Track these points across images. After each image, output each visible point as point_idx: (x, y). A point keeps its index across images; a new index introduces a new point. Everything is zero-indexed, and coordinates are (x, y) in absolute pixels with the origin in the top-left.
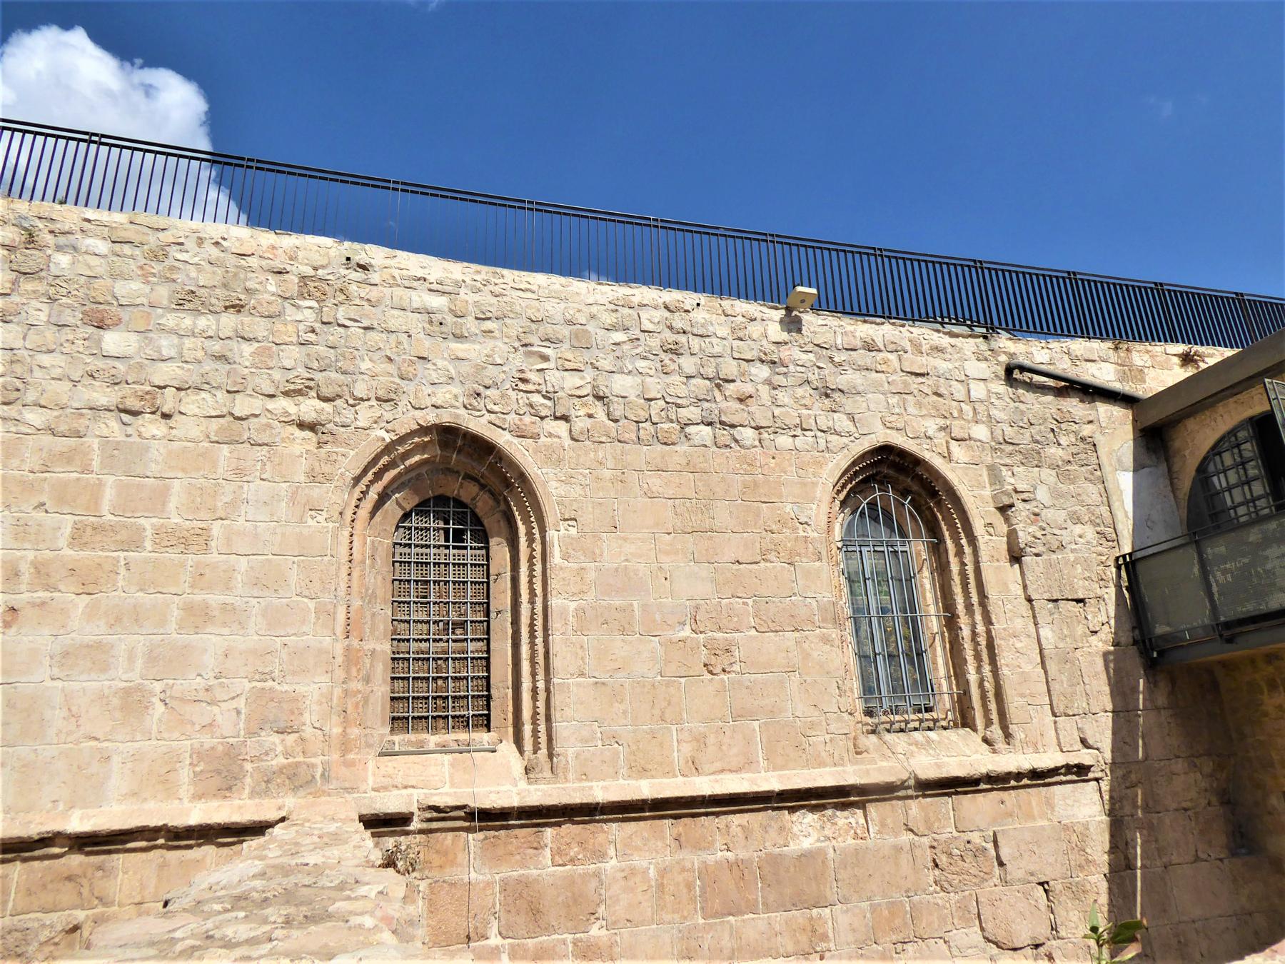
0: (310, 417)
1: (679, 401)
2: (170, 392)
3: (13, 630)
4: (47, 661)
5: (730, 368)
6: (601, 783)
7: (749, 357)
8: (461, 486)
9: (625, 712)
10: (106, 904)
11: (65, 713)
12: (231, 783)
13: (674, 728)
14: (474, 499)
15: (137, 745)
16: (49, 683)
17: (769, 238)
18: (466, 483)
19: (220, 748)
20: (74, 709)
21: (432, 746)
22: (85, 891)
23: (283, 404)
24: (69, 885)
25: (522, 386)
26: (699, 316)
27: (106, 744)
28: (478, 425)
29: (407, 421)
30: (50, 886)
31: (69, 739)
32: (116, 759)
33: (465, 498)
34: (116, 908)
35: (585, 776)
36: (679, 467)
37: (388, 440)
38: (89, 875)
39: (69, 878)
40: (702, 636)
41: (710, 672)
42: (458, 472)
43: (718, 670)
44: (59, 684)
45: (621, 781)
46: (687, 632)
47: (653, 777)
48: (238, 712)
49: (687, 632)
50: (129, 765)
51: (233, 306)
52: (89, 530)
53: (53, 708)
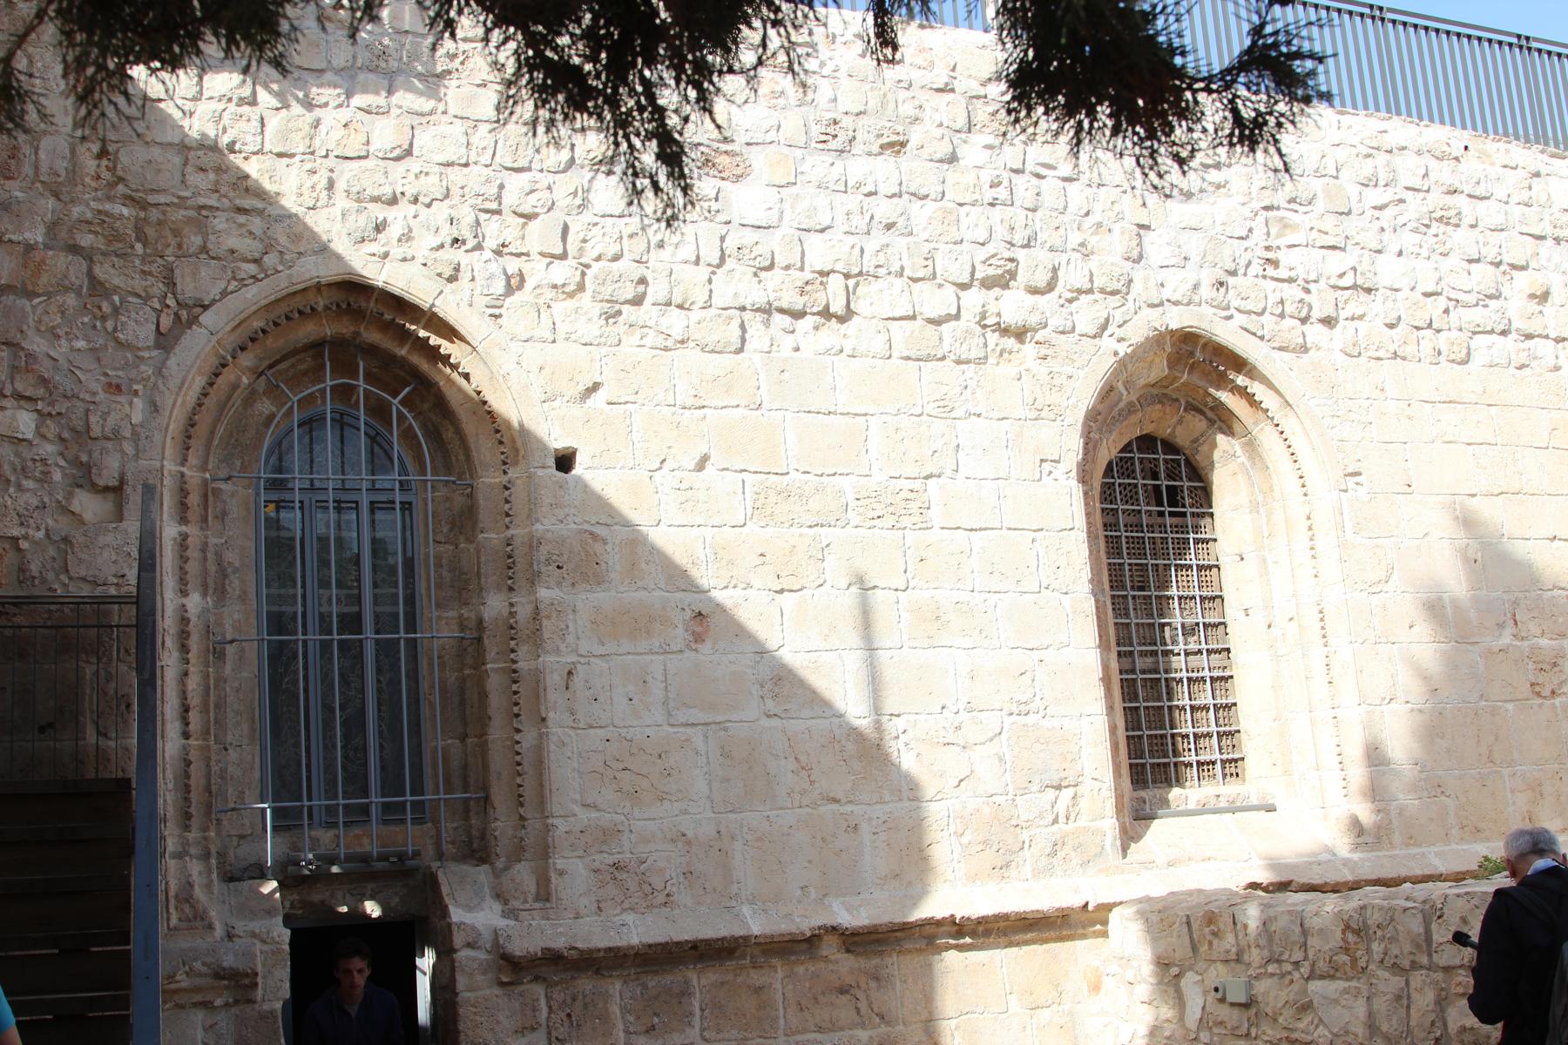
0: (1011, 318)
1: (1461, 296)
2: (836, 282)
3: (705, 648)
4: (755, 689)
5: (1518, 249)
6: (1432, 849)
7: (1538, 233)
8: (1180, 422)
9: (1448, 751)
10: (888, 1023)
11: (792, 765)
12: (1009, 858)
13: (1506, 772)
14: (1195, 441)
15: (887, 808)
16: (765, 722)
17: (1367, 11)
18: (1189, 417)
19: (987, 810)
20: (803, 758)
21: (1192, 806)
22: (863, 1006)
23: (974, 299)
24: (845, 998)
25: (1270, 271)
26: (1470, 165)
27: (849, 808)
28: (1229, 334)
29: (1140, 327)
30: (821, 999)
31: (804, 802)
32: (865, 828)
33: (1182, 439)
34: (901, 1027)
35: (1410, 840)
36: (1473, 398)
37: (1122, 354)
38: (863, 985)
39: (843, 990)
40: (1526, 643)
41: (1538, 694)
42: (1177, 400)
43: (1546, 692)
44: (776, 722)
45: (1454, 846)
46: (1506, 639)
47: (1488, 839)
48: (1001, 760)
49: (1506, 639)
50: (883, 836)
51: (891, 145)
52: (772, 493)
53: (777, 757)
